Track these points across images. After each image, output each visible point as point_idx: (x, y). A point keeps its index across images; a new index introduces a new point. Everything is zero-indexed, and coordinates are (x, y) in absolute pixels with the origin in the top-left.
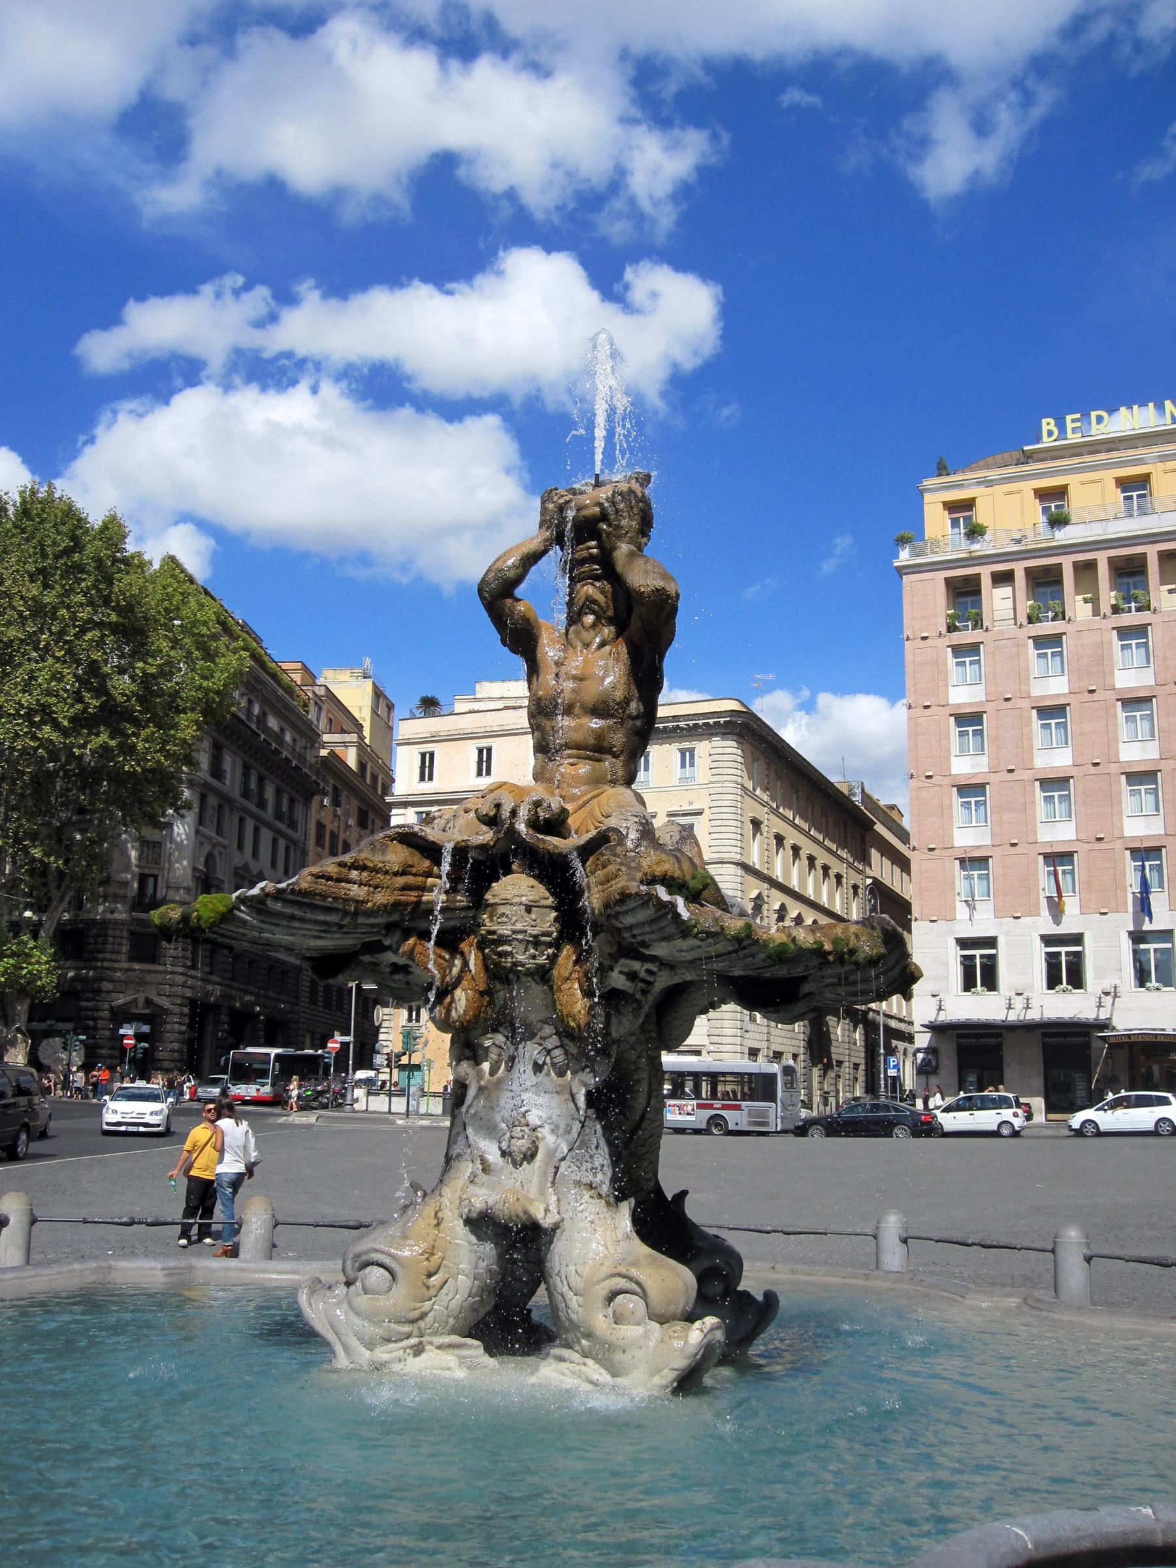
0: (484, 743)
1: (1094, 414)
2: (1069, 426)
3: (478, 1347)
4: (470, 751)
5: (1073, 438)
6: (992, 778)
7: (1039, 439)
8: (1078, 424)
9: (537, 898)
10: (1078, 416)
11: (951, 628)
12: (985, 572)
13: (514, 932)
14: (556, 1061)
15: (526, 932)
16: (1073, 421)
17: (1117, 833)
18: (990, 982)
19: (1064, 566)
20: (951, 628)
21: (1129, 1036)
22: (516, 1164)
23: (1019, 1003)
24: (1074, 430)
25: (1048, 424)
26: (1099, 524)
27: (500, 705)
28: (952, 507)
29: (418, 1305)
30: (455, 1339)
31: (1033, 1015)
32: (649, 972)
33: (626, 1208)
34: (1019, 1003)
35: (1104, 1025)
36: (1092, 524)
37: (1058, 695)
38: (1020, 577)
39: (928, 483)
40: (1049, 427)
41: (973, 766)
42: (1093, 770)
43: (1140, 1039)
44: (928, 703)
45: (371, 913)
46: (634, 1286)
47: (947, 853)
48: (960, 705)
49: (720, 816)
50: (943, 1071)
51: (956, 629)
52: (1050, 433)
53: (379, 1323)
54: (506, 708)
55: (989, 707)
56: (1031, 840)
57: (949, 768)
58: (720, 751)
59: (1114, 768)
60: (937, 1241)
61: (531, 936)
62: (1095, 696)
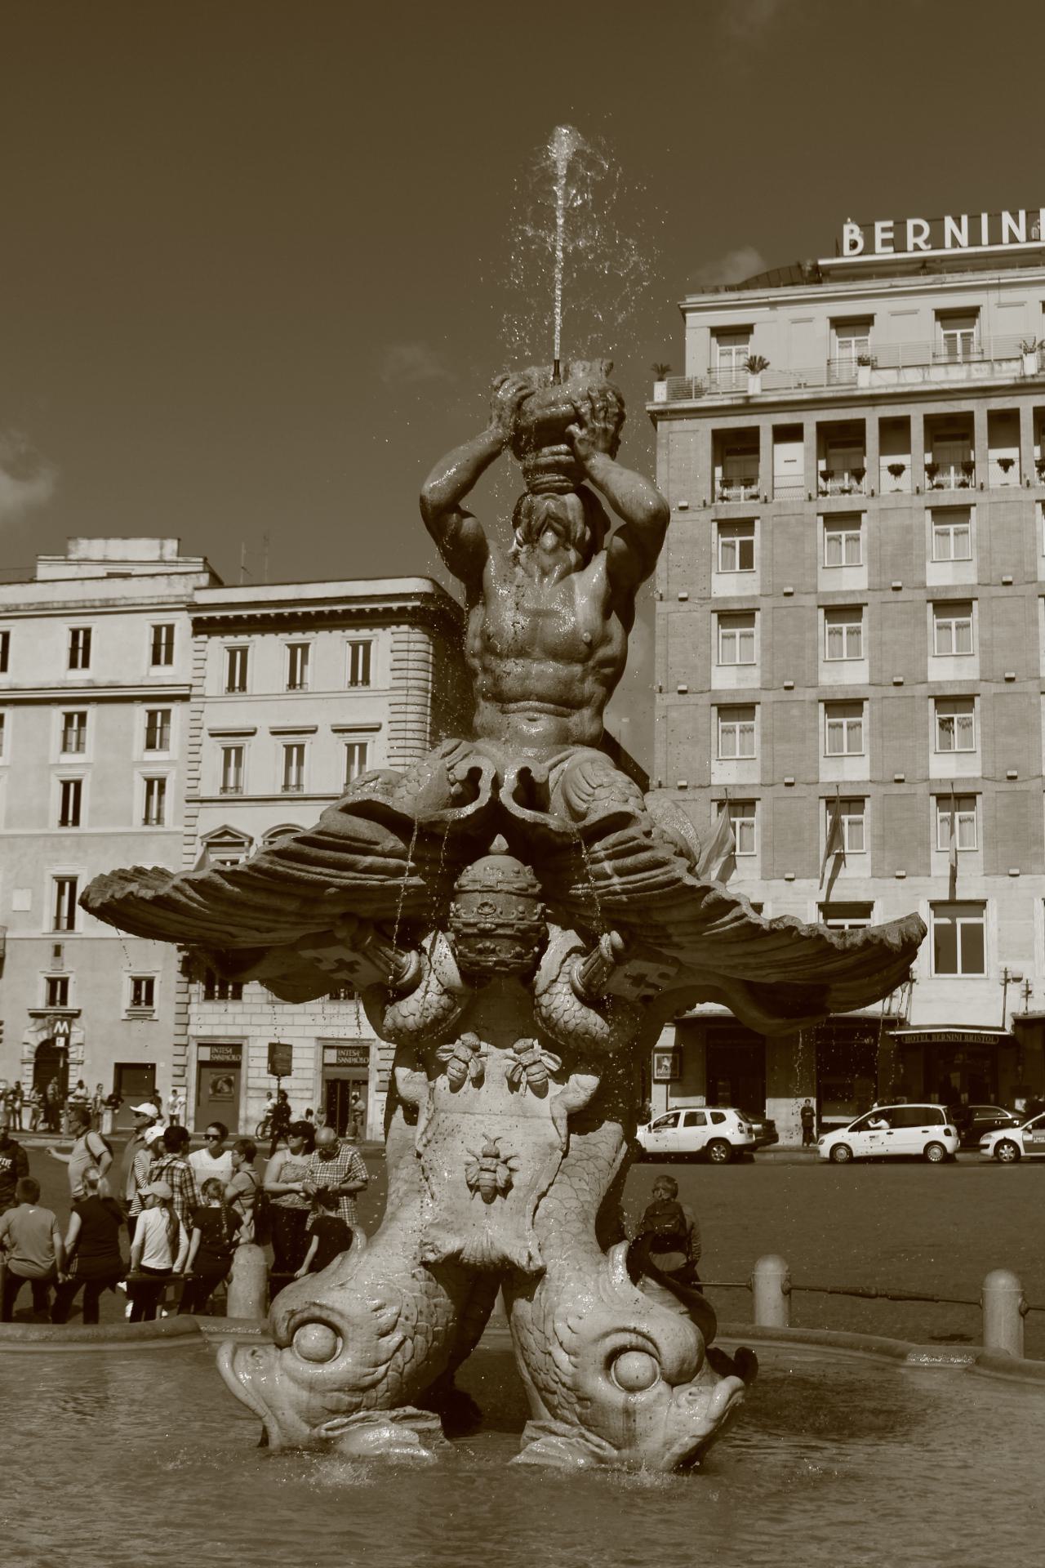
0: (80, 622)
1: (911, 223)
2: (879, 236)
3: (434, 1419)
4: (59, 633)
5: (884, 254)
6: (765, 697)
7: (838, 253)
8: (890, 235)
9: (524, 885)
10: (890, 224)
12: (766, 423)
13: (499, 926)
14: (532, 1078)
15: (512, 925)
16: (884, 230)
17: (919, 775)
19: (867, 423)
21: (930, 1035)
22: (488, 1199)
24: (885, 243)
25: (851, 231)
26: (915, 370)
27: (101, 571)
28: (723, 334)
29: (372, 1370)
30: (410, 1410)
32: (663, 976)
37: (853, 592)
38: (810, 432)
39: (691, 300)
41: (739, 680)
42: (893, 691)
43: (943, 1039)
44: (684, 595)
45: (333, 900)
46: (640, 1341)
47: (701, 794)
48: (726, 600)
49: (402, 734)
52: (854, 245)
53: (323, 1393)
54: (110, 576)
55: (764, 604)
56: (811, 778)
57: (709, 680)
58: (404, 646)
60: (831, 1293)
61: (518, 930)
62: (901, 596)
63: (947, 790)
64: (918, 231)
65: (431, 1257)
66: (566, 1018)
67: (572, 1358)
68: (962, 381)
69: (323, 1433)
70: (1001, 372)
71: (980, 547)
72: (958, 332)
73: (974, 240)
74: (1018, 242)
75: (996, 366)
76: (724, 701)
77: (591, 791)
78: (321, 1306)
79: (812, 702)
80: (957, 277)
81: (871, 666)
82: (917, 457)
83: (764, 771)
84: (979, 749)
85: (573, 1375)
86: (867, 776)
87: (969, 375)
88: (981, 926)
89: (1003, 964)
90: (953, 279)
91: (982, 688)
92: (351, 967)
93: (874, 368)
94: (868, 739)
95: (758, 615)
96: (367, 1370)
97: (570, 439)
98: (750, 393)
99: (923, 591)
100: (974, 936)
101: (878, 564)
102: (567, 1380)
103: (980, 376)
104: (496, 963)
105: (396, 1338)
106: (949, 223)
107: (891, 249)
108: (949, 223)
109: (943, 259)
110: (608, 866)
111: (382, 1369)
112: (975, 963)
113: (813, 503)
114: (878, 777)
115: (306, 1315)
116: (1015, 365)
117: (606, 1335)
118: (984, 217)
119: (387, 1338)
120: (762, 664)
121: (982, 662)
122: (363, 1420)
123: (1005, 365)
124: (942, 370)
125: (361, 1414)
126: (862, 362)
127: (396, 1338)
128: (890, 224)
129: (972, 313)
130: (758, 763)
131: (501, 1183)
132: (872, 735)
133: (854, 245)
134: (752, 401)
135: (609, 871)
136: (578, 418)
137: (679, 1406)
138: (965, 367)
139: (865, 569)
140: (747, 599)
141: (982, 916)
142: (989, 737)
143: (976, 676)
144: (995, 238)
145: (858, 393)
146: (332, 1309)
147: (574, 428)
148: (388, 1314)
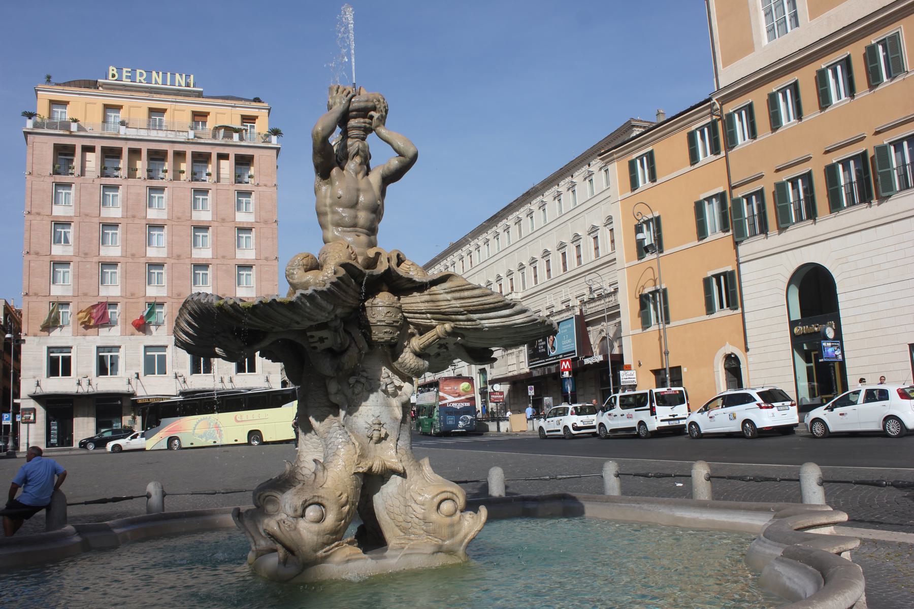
1: (138, 71)
2: (125, 74)
5: (126, 82)
8: (130, 74)
11: (56, 172)
13: (394, 322)
15: (398, 322)
16: (127, 72)
18: (67, 372)
20: (56, 172)
21: (149, 399)
23: (84, 383)
26: (144, 130)
31: (91, 390)
33: (426, 462)
34: (84, 383)
35: (133, 395)
36: (141, 130)
37: (115, 218)
40: (113, 72)
47: (45, 299)
50: (37, 421)
51: (59, 174)
52: (113, 76)
55: (76, 220)
59: (143, 260)
63: (153, 301)
64: (141, 75)
65: (361, 470)
66: (411, 363)
67: (423, 507)
68: (164, 137)
69: (324, 554)
70: (179, 136)
71: (168, 204)
72: (158, 118)
73: (164, 83)
74: (181, 86)
75: (178, 134)
76: (57, 259)
77: (408, 267)
78: (318, 497)
79: (96, 263)
80: (158, 96)
81: (122, 249)
82: (141, 165)
83: (74, 291)
84: (166, 285)
85: (424, 513)
86: (119, 294)
87: (167, 136)
88: (165, 355)
89: (175, 371)
90: (156, 97)
91: (168, 261)
92: (322, 340)
93: (127, 127)
94: (120, 279)
95: (72, 224)
96: (337, 523)
97: (371, 117)
98: (72, 130)
99: (144, 220)
100: (162, 359)
101: (126, 207)
102: (420, 516)
103: (171, 136)
104: (392, 338)
105: (347, 508)
106: (154, 74)
107: (130, 80)
108: (154, 74)
109: (152, 88)
110: (449, 296)
111: (343, 521)
112: (163, 371)
113: (99, 180)
114: (124, 295)
115: (311, 502)
116: (185, 134)
117: (437, 495)
118: (169, 74)
119: (344, 508)
120: (74, 245)
121: (168, 250)
122: (337, 546)
123: (181, 133)
124: (155, 132)
125: (336, 543)
126: (123, 123)
127: (347, 507)
128: (130, 70)
129: (163, 111)
130: (71, 288)
131: (383, 436)
132: (121, 277)
133: (113, 76)
134: (73, 134)
135: (449, 298)
136: (374, 109)
137: (467, 521)
138: (165, 132)
139: (120, 209)
140: (67, 217)
141: (165, 351)
142: (171, 280)
143: (165, 255)
144: (173, 84)
145: (120, 136)
146: (323, 498)
147: (372, 113)
148: (344, 498)
